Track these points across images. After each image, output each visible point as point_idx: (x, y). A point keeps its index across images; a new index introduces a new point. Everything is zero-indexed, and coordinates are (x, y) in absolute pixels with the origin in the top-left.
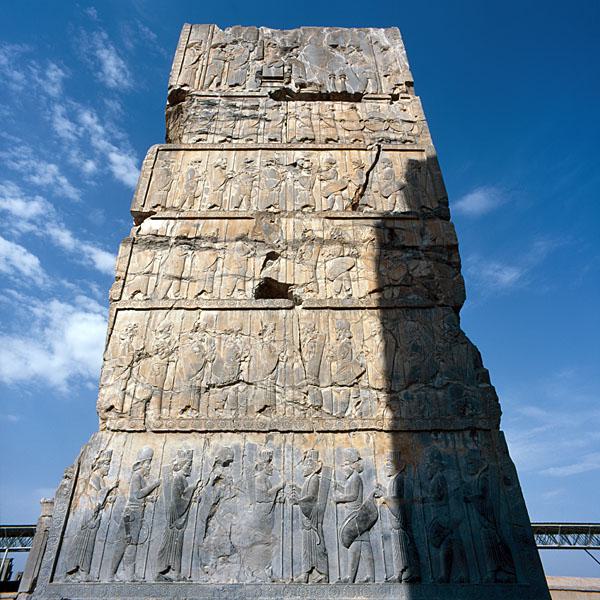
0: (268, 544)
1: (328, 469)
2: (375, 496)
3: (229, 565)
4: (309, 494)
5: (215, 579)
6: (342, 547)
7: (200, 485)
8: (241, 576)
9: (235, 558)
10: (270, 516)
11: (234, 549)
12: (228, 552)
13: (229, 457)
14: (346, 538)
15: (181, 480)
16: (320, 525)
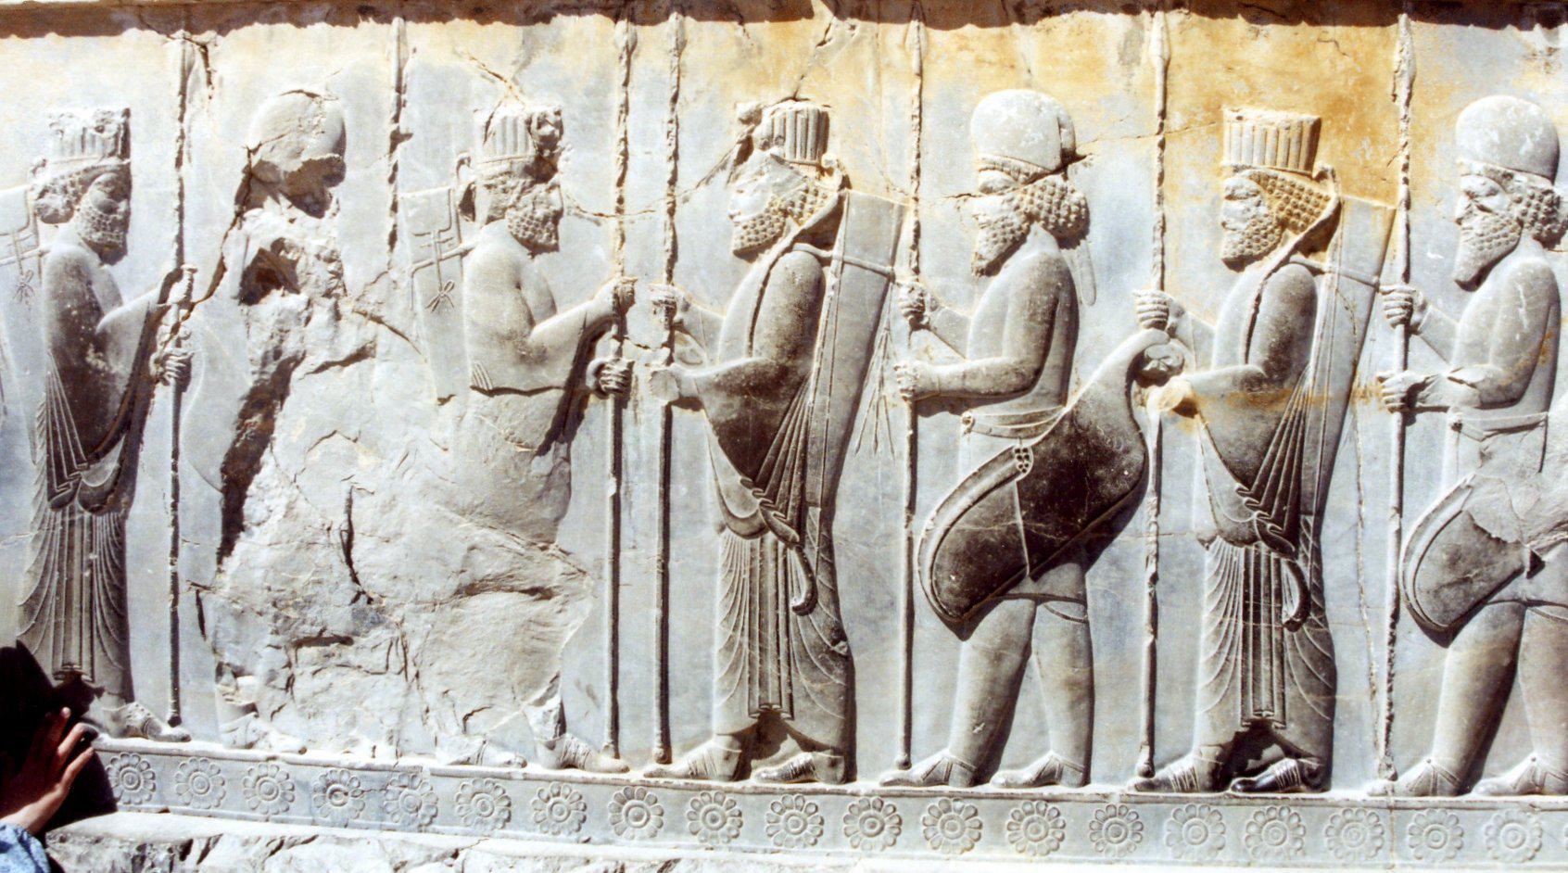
0: (540, 593)
1: (879, 210)
2: (1141, 373)
3: (353, 676)
4: (763, 355)
5: (281, 737)
6: (930, 626)
7: (177, 292)
8: (414, 732)
9: (372, 648)
10: (542, 465)
11: (368, 608)
12: (338, 618)
13: (316, 148)
14: (951, 582)
15: (77, 270)
16: (814, 513)
